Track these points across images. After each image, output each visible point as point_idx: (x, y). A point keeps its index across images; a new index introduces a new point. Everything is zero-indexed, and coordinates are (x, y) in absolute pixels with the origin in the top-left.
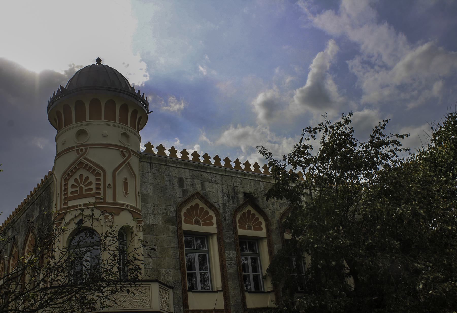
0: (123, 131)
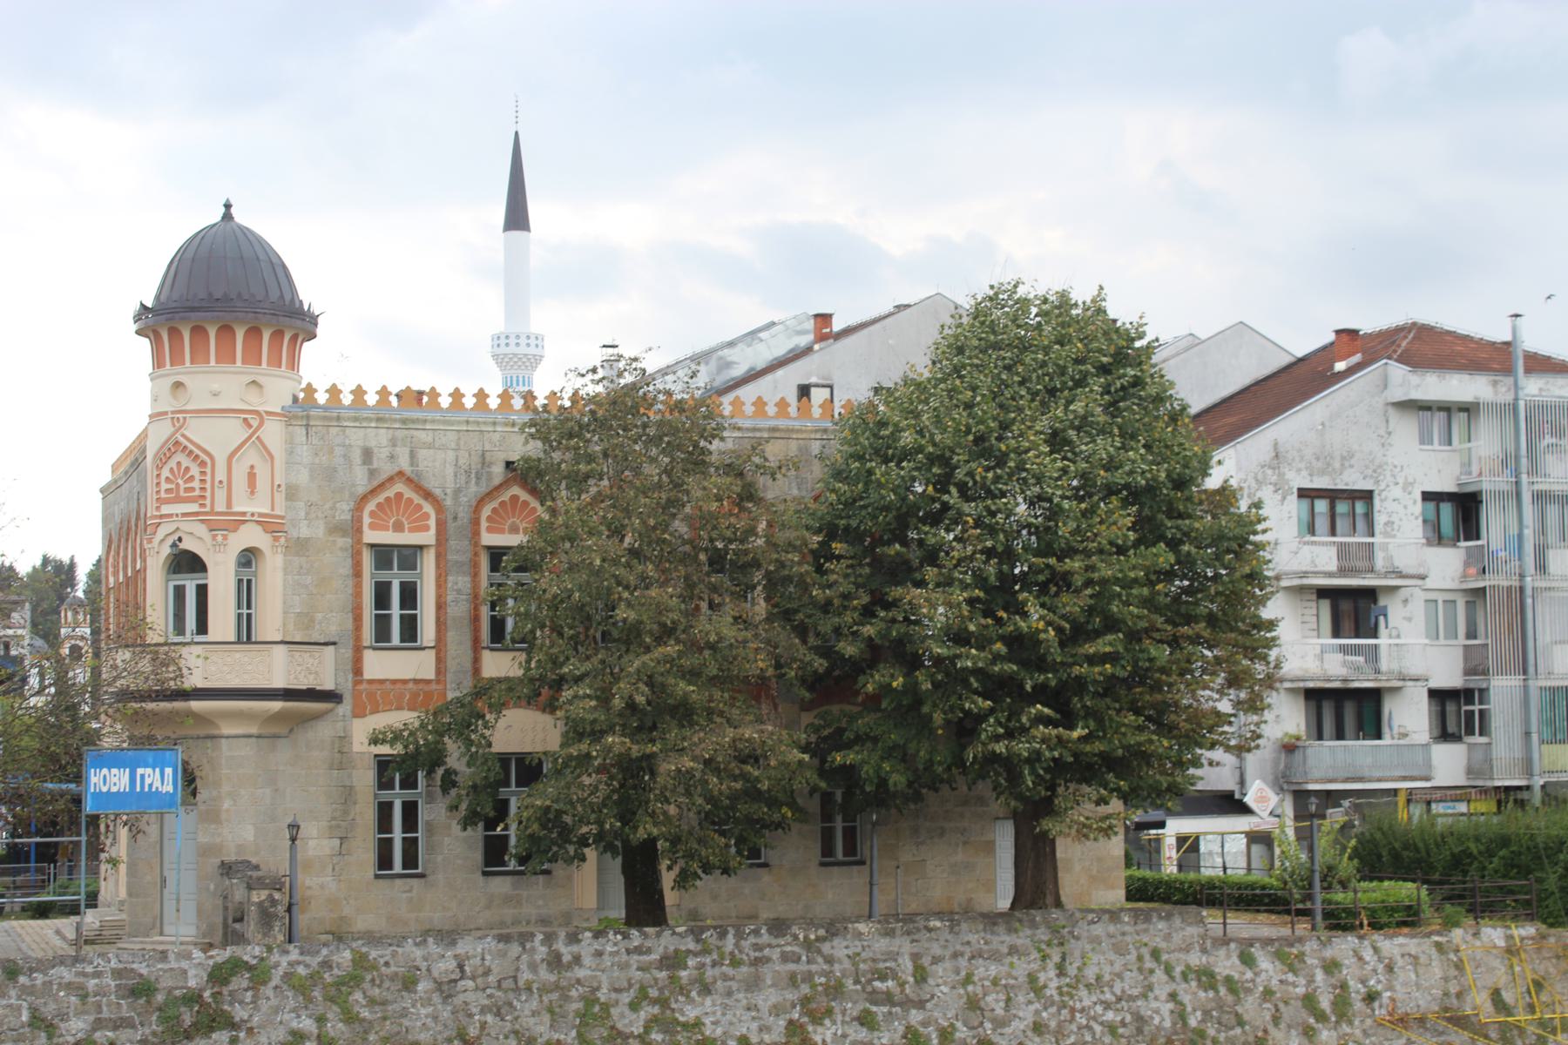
0: (250, 378)
